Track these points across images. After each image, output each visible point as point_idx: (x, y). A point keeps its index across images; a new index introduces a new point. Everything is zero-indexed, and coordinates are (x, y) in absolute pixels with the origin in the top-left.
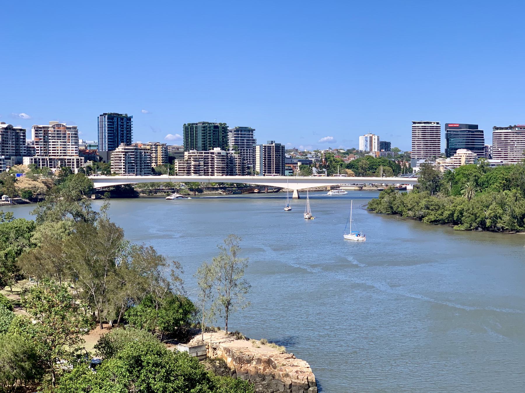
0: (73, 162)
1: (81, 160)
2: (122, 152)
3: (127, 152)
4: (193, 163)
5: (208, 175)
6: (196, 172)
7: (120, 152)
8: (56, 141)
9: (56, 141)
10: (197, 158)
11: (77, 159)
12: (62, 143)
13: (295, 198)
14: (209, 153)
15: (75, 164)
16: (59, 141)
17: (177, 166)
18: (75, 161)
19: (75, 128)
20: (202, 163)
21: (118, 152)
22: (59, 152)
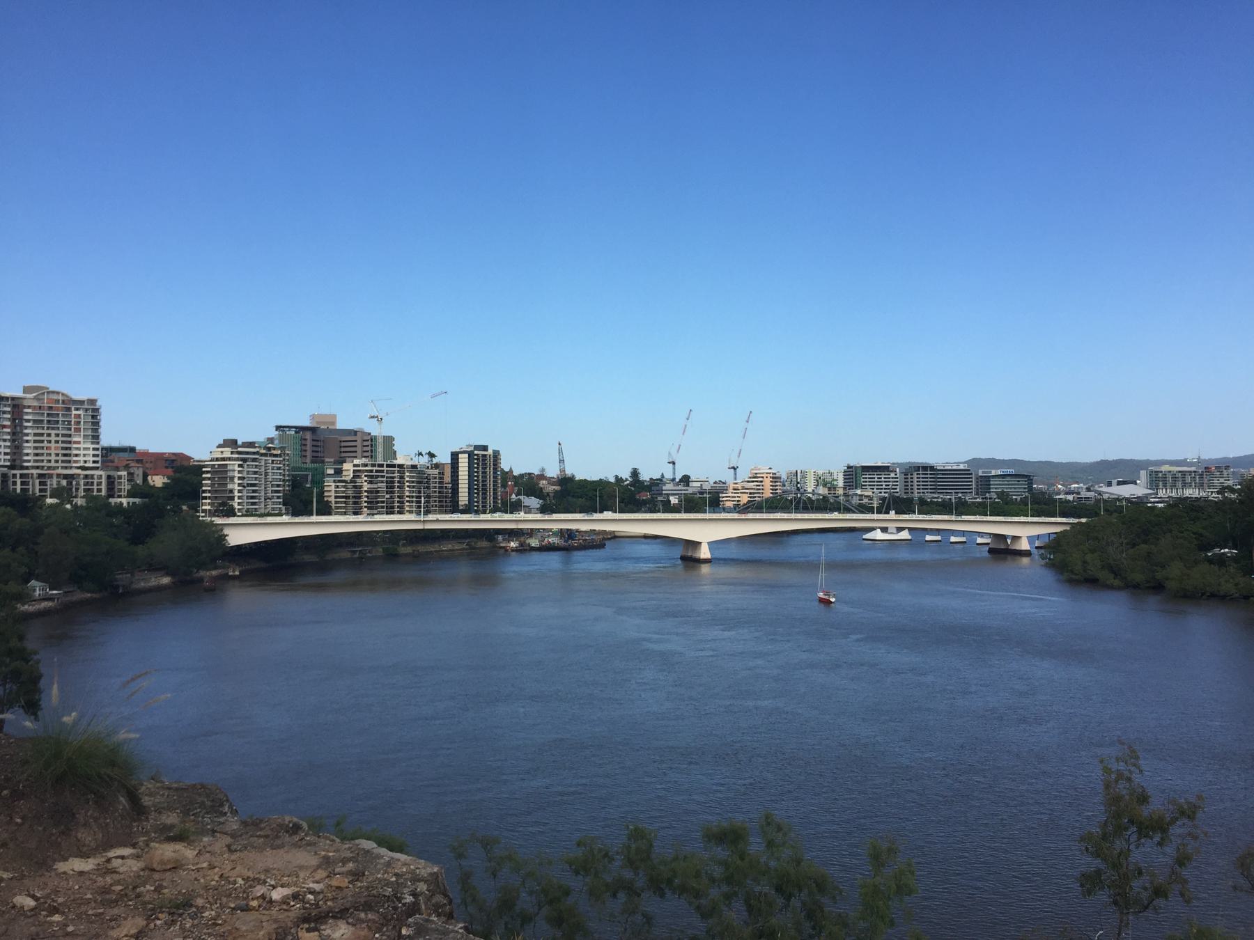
0: (99, 484)
1: (120, 477)
2: (237, 459)
3: (245, 460)
4: (366, 487)
5: (392, 513)
6: (374, 505)
7: (230, 459)
8: (45, 431)
9: (45, 431)
10: (372, 477)
11: (109, 477)
12: (60, 439)
13: (706, 561)
14: (394, 466)
15: (104, 487)
16: (53, 432)
17: (333, 494)
18: (104, 480)
19: (93, 402)
20: (382, 486)
21: (223, 459)
22: (53, 458)
